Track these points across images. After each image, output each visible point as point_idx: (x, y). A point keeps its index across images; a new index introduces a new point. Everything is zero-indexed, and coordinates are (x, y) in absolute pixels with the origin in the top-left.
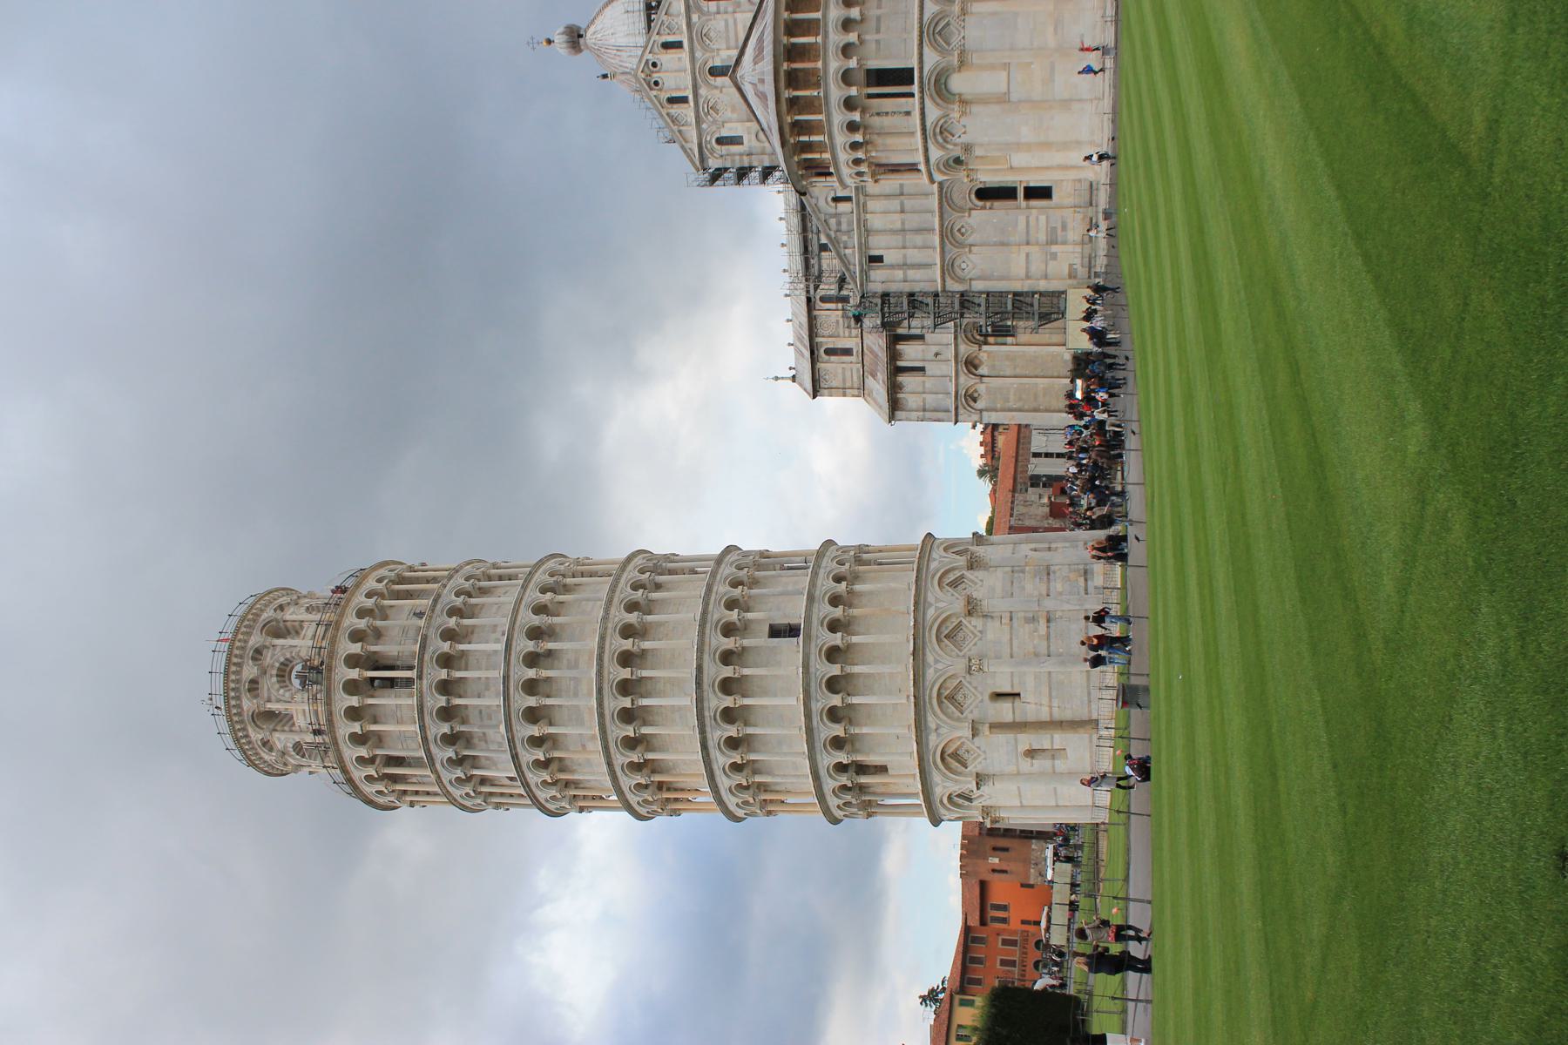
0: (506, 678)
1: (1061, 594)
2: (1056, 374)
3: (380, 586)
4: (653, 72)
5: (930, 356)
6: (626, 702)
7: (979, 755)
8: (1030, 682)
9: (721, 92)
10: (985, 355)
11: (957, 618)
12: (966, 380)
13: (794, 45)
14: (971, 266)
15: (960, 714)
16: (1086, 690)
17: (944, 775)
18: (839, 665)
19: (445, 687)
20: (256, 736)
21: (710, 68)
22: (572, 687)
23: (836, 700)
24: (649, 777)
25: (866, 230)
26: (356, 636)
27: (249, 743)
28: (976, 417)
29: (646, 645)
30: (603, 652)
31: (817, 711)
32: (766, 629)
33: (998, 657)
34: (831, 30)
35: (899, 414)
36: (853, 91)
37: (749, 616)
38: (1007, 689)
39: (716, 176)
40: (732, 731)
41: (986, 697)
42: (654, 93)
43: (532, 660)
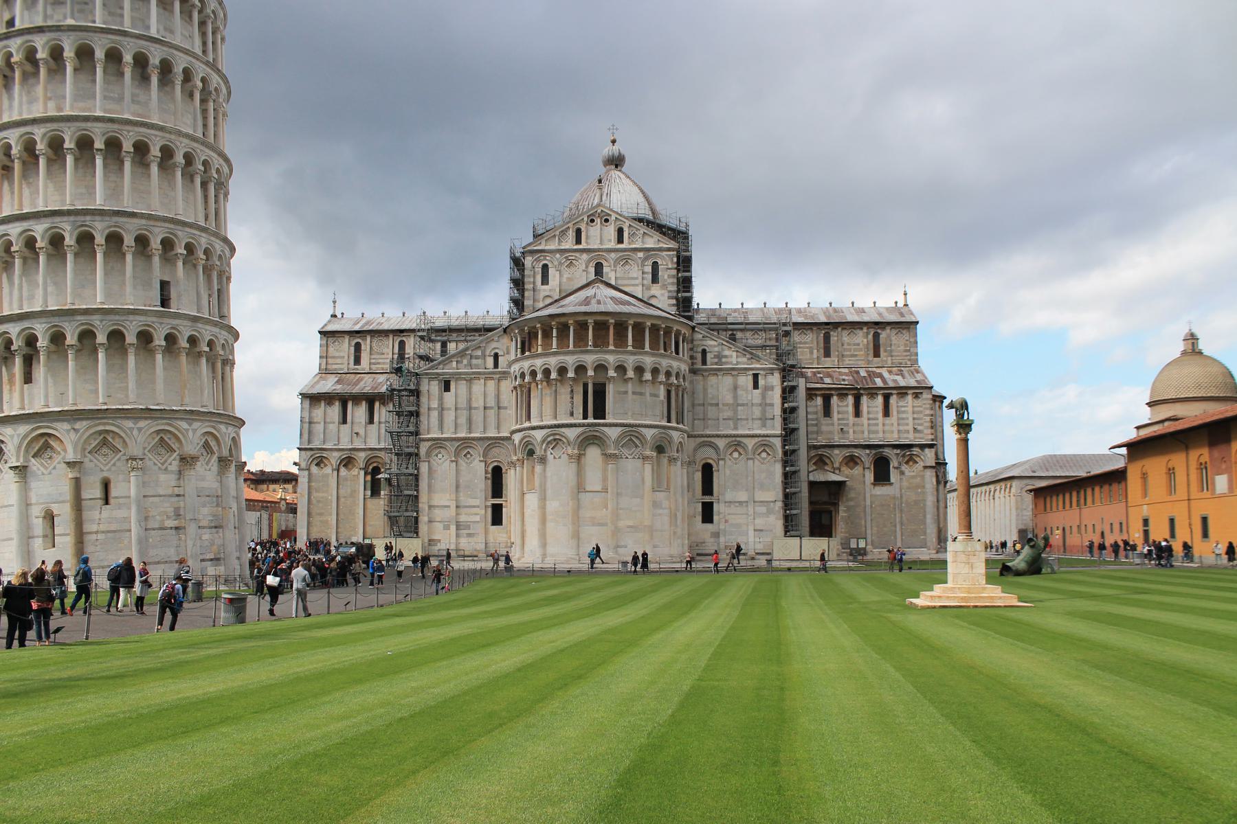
0: (124, 34)
1: (200, 538)
2: (339, 530)
4: (601, 219)
6: (99, 144)
7: (46, 468)
8: (121, 513)
9: (584, 271)
10: (356, 473)
11: (179, 449)
12: (335, 457)
13: (627, 329)
14: (443, 459)
17: (26, 436)
21: (602, 264)
22: (112, 95)
23: (101, 338)
25: (471, 379)
28: (303, 465)
30: (148, 128)
32: (166, 279)
34: (636, 357)
35: (307, 402)
36: (591, 373)
37: (180, 264)
38: (114, 492)
39: (517, 263)
40: (69, 240)
41: (105, 474)
42: (586, 219)
43: (141, 61)
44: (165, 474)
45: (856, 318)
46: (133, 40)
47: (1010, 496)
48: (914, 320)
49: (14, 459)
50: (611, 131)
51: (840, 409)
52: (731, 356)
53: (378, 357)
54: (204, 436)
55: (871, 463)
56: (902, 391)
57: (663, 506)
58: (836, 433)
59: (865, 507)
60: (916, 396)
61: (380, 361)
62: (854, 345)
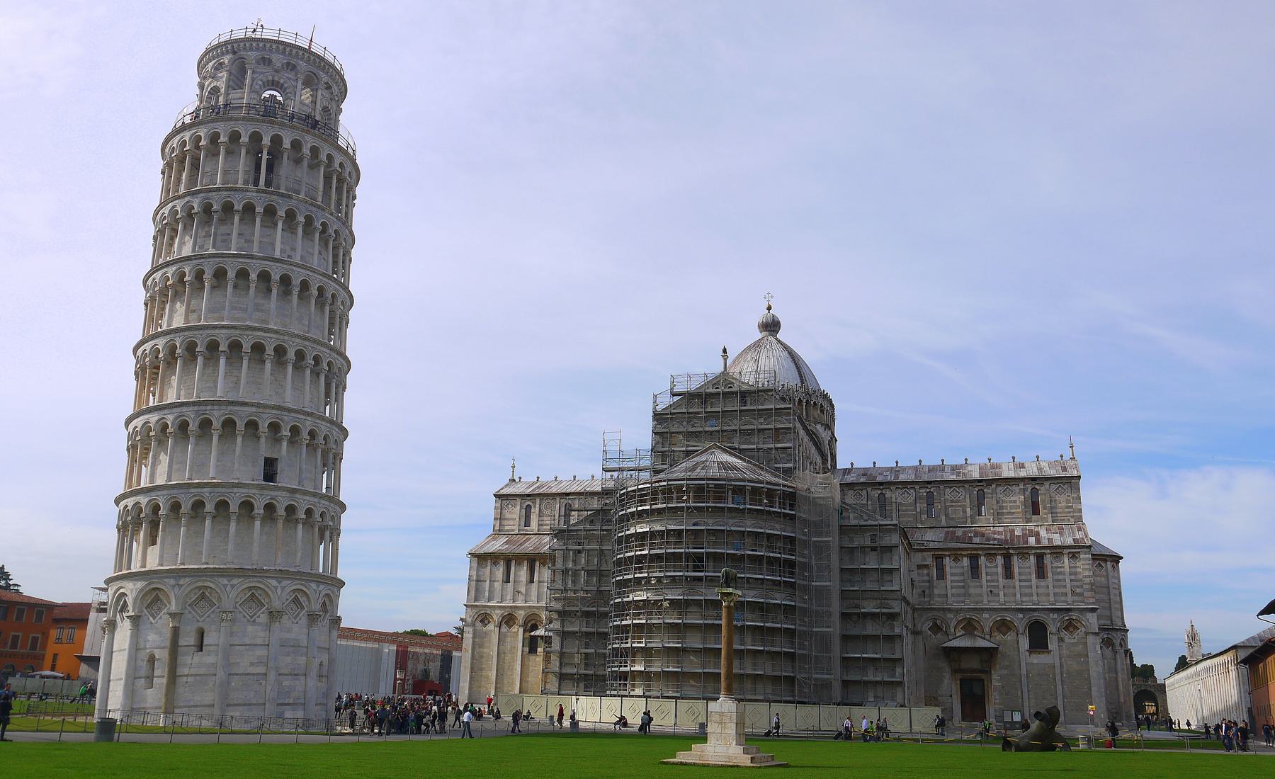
0: (251, 257)
3: (337, 165)
8: (210, 659)
11: (268, 603)
15: (189, 603)
16: (198, 704)
17: (142, 590)
18: (237, 511)
19: (249, 209)
20: (226, 60)
22: (241, 306)
23: (209, 507)
26: (296, 145)
29: (268, 365)
31: (201, 493)
33: (232, 634)
37: (285, 444)
38: (205, 643)
40: (193, 426)
41: (200, 624)
43: (264, 277)
44: (253, 625)
45: (1012, 474)
46: (258, 261)
48: (1075, 473)
51: (989, 570)
54: (294, 593)
55: (1025, 628)
56: (1057, 551)
58: (985, 597)
60: (1074, 556)
62: (1011, 502)
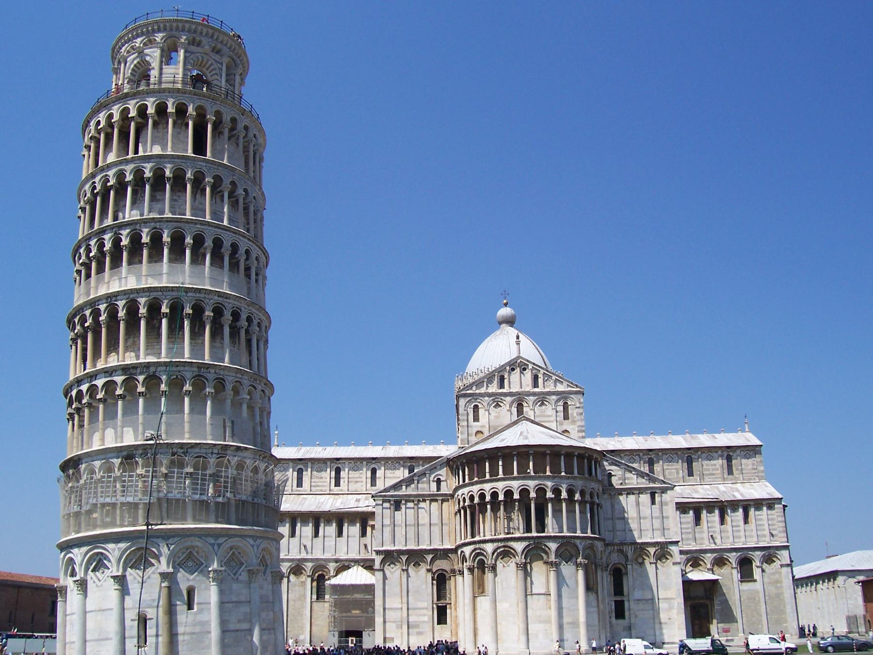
4: (520, 368)
5: (304, 541)
9: (508, 410)
11: (246, 562)
12: (286, 566)
15: (177, 563)
24: (123, 320)
27: (154, 31)
36: (533, 495)
41: (191, 583)
42: (508, 368)
47: (833, 587)
49: (115, 568)
50: (504, 296)
52: (632, 478)
53: (318, 480)
56: (758, 504)
57: (593, 605)
59: (735, 600)
61: (319, 484)
